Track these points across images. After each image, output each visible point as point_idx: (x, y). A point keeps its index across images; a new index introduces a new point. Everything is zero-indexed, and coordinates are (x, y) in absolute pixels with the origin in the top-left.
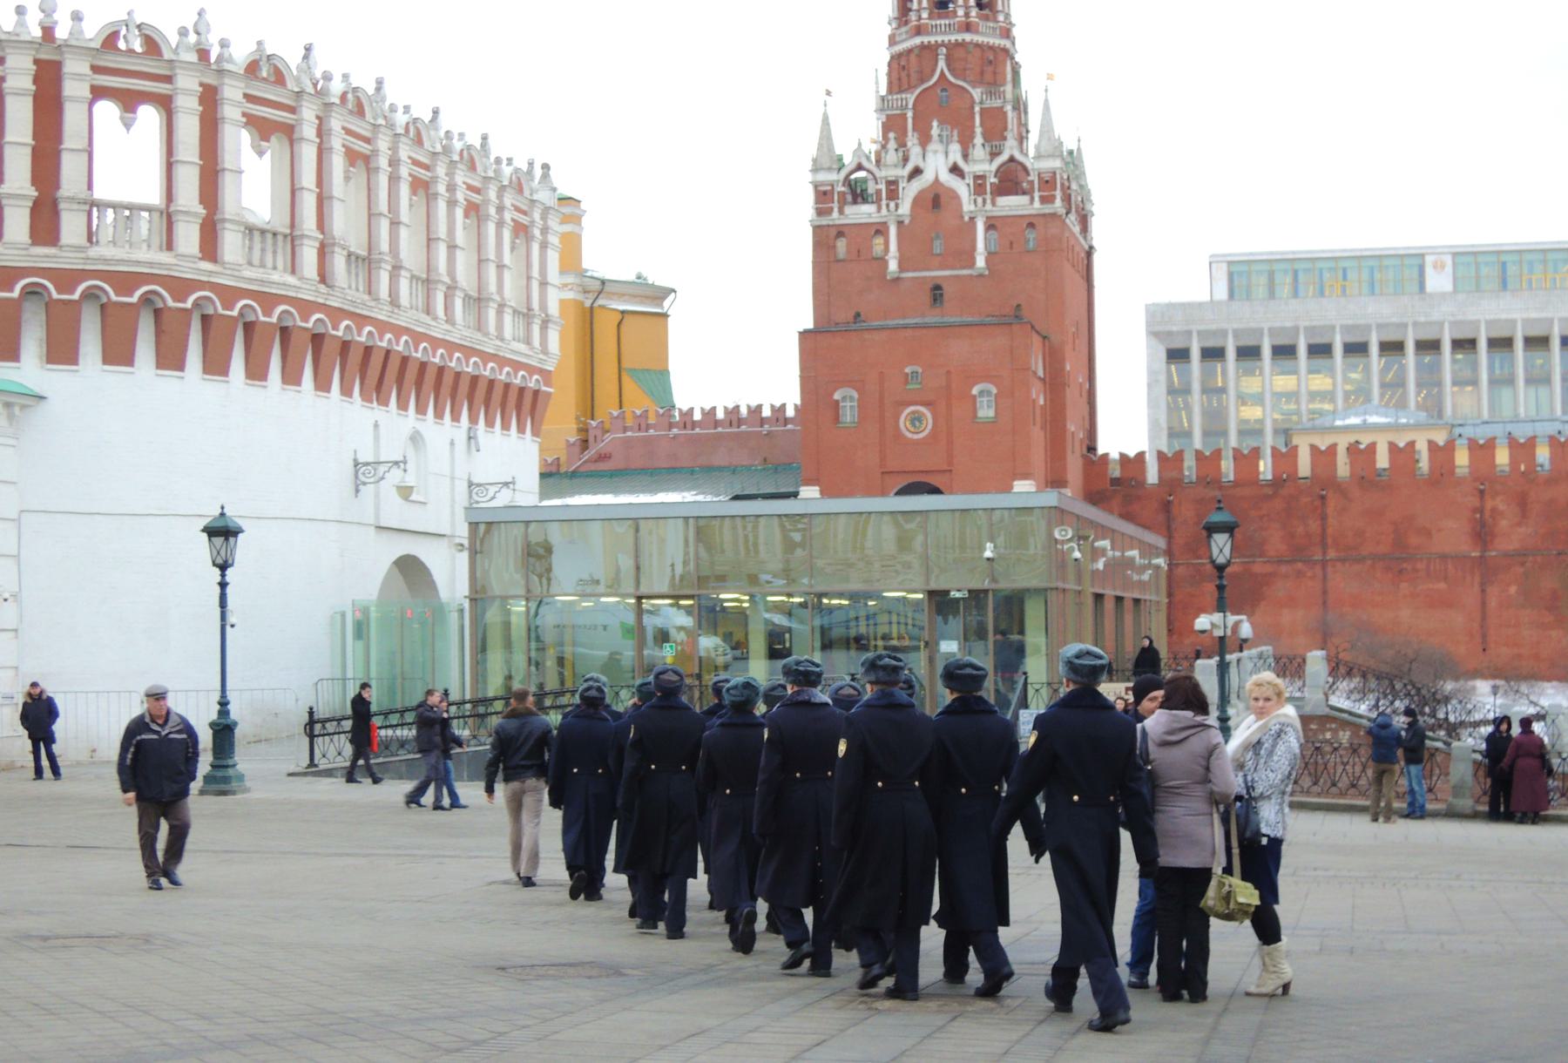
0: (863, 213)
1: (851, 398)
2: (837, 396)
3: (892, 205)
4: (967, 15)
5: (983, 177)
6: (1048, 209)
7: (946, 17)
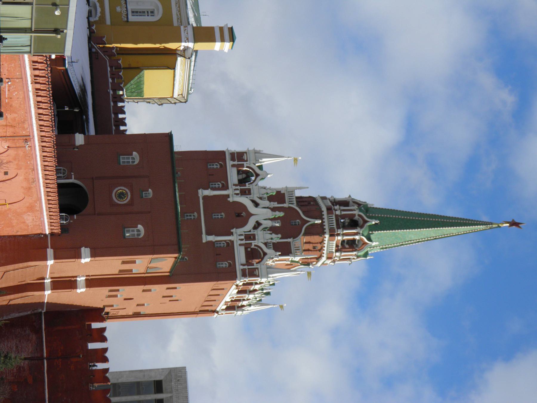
0: (233, 176)
1: (134, 162)
2: (134, 153)
3: (238, 192)
4: (338, 235)
5: (254, 239)
6: (239, 273)
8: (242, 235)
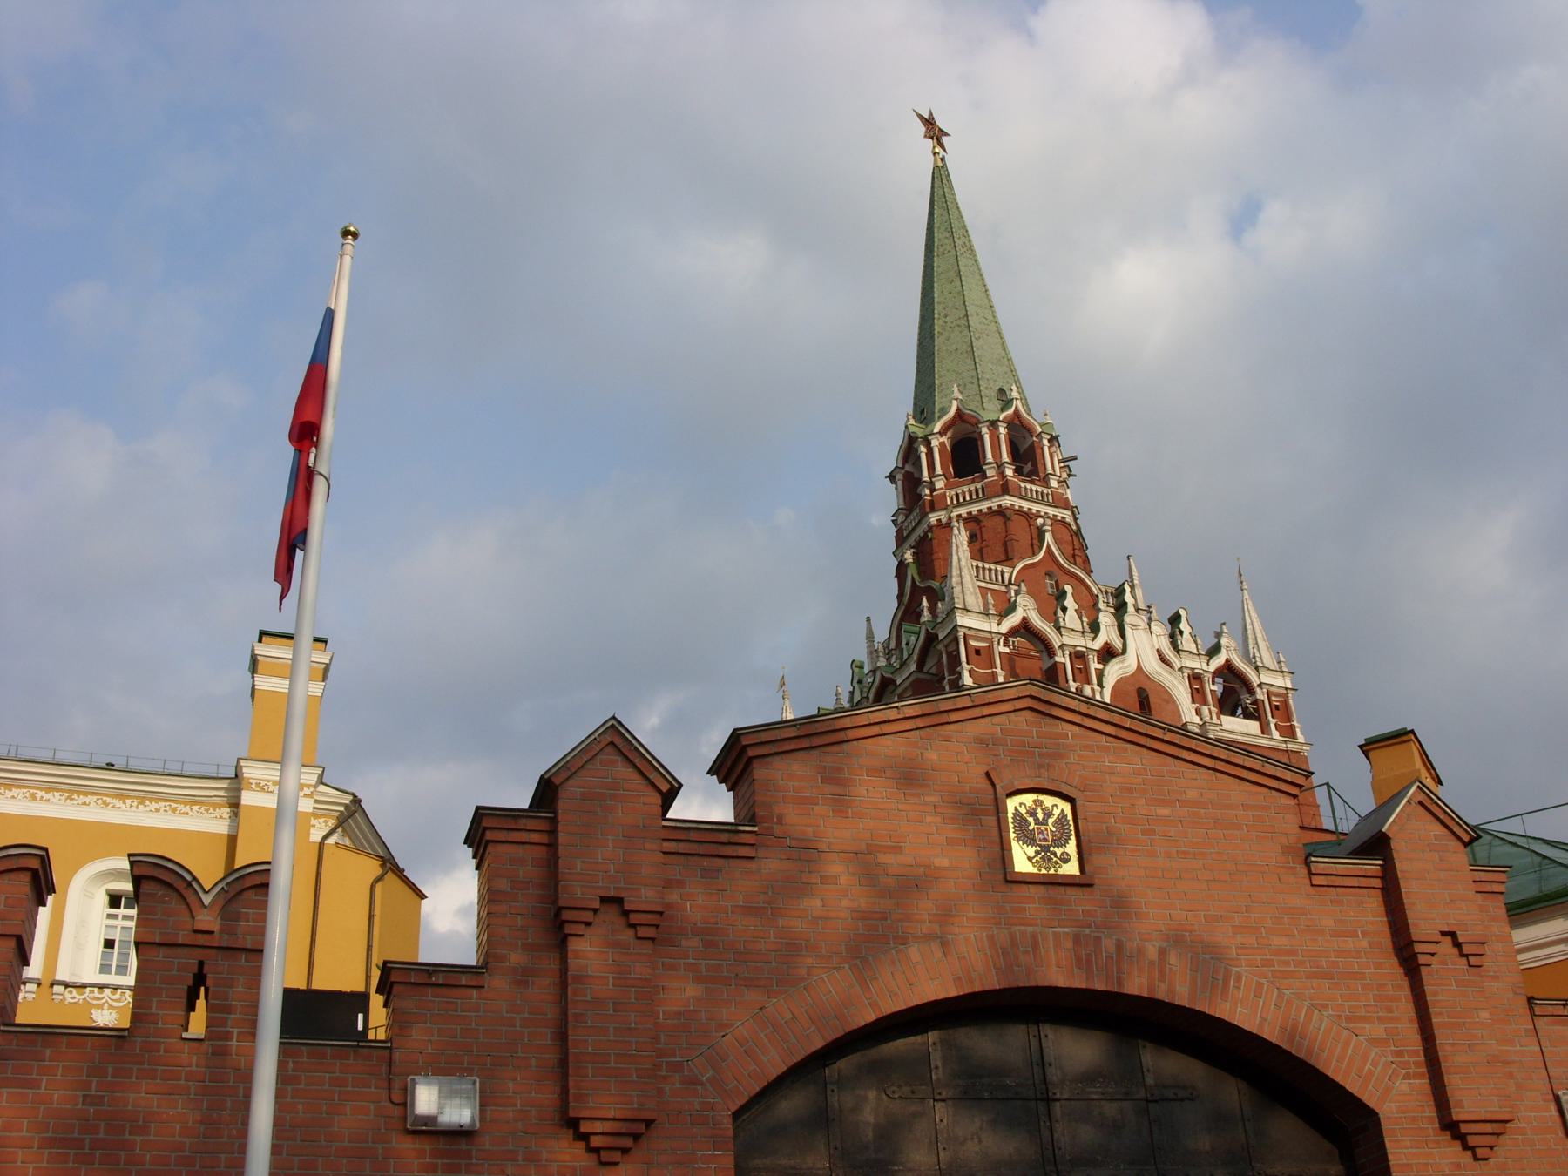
7: (1032, 482)
8: (1198, 712)
